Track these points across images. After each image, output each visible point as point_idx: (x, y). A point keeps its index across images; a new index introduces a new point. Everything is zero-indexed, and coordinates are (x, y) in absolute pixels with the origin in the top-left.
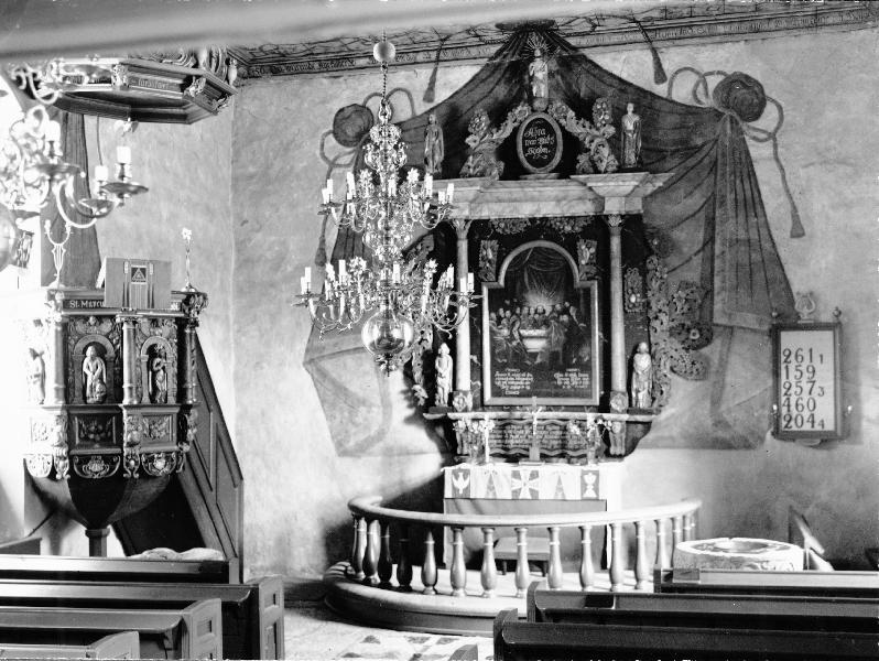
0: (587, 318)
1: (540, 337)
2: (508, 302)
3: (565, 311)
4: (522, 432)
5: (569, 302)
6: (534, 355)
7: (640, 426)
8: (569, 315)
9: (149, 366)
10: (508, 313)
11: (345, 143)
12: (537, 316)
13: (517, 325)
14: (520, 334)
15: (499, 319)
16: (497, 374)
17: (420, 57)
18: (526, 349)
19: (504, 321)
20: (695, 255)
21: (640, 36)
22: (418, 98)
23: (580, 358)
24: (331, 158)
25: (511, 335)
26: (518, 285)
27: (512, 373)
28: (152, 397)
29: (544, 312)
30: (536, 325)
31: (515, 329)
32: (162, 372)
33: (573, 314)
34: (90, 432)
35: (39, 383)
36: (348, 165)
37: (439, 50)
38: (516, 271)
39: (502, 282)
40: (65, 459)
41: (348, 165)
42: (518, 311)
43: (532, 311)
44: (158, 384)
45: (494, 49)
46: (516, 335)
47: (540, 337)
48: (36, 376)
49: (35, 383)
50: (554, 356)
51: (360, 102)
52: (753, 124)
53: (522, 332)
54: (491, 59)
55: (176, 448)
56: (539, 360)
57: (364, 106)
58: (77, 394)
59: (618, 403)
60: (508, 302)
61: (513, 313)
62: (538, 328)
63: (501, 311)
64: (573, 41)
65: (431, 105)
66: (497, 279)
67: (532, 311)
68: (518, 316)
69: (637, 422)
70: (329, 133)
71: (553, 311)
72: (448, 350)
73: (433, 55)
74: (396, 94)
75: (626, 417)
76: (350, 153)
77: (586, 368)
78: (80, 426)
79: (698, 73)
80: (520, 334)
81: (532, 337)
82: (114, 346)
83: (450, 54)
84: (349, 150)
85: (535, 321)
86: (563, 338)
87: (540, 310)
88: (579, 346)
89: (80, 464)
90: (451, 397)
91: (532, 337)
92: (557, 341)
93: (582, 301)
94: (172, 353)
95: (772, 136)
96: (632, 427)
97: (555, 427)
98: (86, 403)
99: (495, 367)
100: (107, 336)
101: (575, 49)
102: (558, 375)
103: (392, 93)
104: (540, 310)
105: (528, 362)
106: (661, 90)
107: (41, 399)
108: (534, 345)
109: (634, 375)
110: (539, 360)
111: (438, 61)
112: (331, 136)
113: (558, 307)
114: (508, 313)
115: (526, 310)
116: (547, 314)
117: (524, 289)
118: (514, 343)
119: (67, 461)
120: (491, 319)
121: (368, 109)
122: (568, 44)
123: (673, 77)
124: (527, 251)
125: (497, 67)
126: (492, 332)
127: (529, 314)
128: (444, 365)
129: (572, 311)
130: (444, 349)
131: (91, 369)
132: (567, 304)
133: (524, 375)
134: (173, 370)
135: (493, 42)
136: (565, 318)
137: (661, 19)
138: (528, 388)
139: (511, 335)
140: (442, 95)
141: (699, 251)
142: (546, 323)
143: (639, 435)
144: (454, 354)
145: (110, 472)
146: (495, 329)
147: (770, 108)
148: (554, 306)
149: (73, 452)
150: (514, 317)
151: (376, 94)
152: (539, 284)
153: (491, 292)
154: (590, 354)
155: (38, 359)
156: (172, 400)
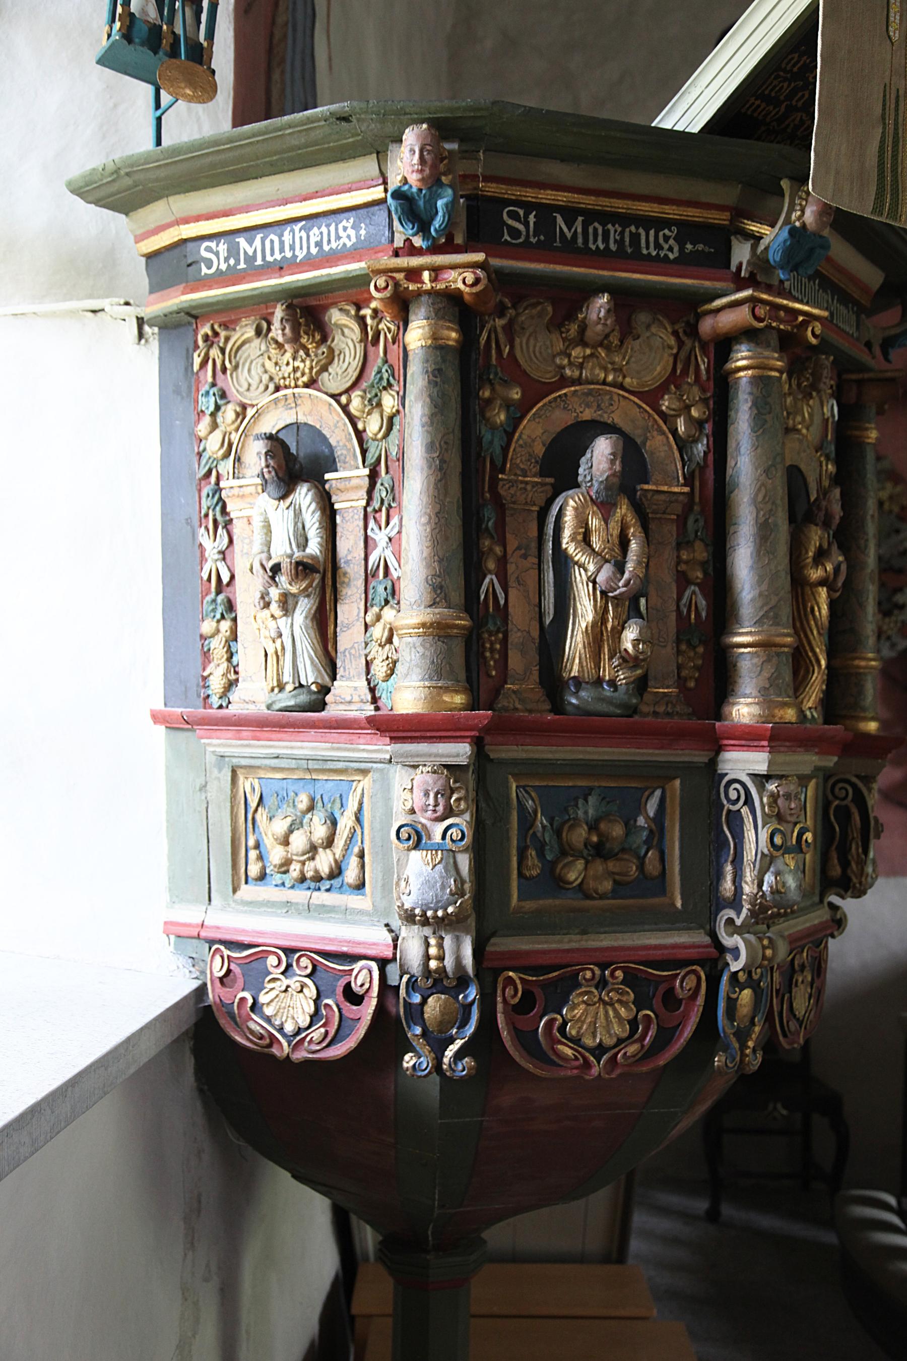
34: (565, 851)
35: (304, 608)
40: (462, 982)
48: (303, 569)
49: (287, 604)
58: (515, 661)
78: (527, 822)
82: (683, 445)
89: (526, 1004)
98: (558, 707)
100: (651, 397)
107: (310, 675)
119: (472, 993)
131: (597, 544)
145: (665, 1037)
149: (501, 944)
155: (304, 495)
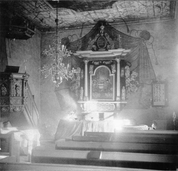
0: (112, 83)
1: (102, 86)
3: (108, 80)
6: (101, 89)
9: (16, 89)
13: (97, 83)
15: (94, 82)
16: (93, 93)
17: (79, 27)
18: (99, 88)
19: (95, 82)
21: (124, 23)
22: (79, 36)
23: (110, 90)
25: (96, 85)
28: (16, 95)
30: (101, 83)
32: (18, 90)
37: (82, 26)
39: (94, 74)
43: (101, 80)
44: (17, 92)
45: (94, 26)
46: (97, 85)
47: (102, 86)
50: (105, 90)
52: (147, 41)
54: (93, 28)
55: (21, 106)
56: (102, 91)
59: (118, 99)
60: (95, 78)
61: (97, 81)
62: (102, 84)
64: (110, 24)
65: (81, 38)
67: (101, 80)
68: (98, 82)
69: (123, 104)
73: (81, 27)
74: (74, 35)
75: (120, 102)
77: (111, 92)
79: (136, 31)
80: (98, 85)
81: (100, 86)
83: (85, 27)
85: (101, 82)
88: (111, 88)
91: (100, 86)
93: (111, 78)
94: (21, 86)
95: (151, 44)
101: (110, 25)
102: (106, 94)
104: (102, 80)
106: (128, 34)
108: (101, 87)
110: (102, 91)
111: (82, 28)
113: (106, 79)
114: (96, 81)
115: (99, 80)
118: (97, 87)
120: (92, 81)
122: (109, 24)
123: (131, 31)
125: (94, 29)
126: (92, 85)
128: (82, 91)
129: (109, 80)
130: (82, 88)
132: (108, 79)
134: (21, 90)
135: (93, 24)
136: (108, 82)
137: (128, 19)
139: (96, 85)
140: (83, 36)
142: (103, 83)
144: (84, 89)
147: (151, 38)
148: (105, 79)
150: (97, 81)
153: (92, 76)
154: (112, 89)
156: (21, 96)
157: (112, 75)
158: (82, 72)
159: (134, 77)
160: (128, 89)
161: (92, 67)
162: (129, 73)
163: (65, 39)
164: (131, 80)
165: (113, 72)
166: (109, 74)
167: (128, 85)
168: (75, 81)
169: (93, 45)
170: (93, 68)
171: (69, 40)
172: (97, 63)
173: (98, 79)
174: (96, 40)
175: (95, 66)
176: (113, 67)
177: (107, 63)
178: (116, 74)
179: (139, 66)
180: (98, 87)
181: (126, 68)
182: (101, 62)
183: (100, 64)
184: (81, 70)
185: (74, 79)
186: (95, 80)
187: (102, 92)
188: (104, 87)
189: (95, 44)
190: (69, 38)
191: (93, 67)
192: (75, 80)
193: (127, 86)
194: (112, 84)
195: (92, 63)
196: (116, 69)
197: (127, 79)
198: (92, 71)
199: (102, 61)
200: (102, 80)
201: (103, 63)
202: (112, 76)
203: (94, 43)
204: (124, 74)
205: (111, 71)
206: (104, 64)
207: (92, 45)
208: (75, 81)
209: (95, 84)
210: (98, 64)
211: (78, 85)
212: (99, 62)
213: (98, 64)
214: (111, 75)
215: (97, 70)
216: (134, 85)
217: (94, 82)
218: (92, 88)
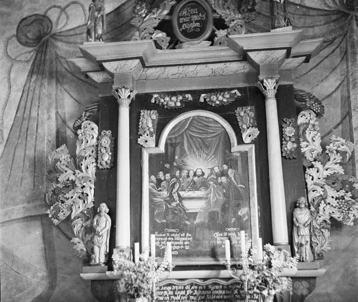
0: (246, 180)
1: (200, 198)
2: (167, 166)
3: (223, 174)
4: (184, 293)
5: (227, 164)
7: (305, 284)
8: (227, 176)
10: (168, 176)
11: (26, 44)
12: (196, 179)
13: (177, 186)
14: (179, 196)
15: (159, 182)
19: (163, 184)
20: (335, 128)
24: (13, 57)
26: (178, 149)
27: (171, 233)
29: (203, 174)
30: (194, 186)
31: (174, 190)
33: (232, 176)
36: (27, 61)
38: (176, 138)
39: (162, 149)
41: (27, 61)
42: (177, 173)
46: (175, 196)
47: (200, 198)
50: (212, 216)
51: (42, 13)
53: (181, 193)
56: (198, 221)
57: (44, 16)
60: (167, 166)
61: (173, 176)
63: (161, 175)
66: (157, 145)
70: (13, 36)
71: (212, 173)
72: (108, 210)
74: (72, 6)
76: (30, 52)
80: (179, 196)
84: (31, 49)
85: (194, 183)
86: (221, 198)
87: (199, 173)
88: (238, 206)
90: (109, 255)
92: (216, 202)
96: (297, 283)
97: (217, 287)
99: (154, 228)
103: (68, 5)
104: (199, 173)
105: (187, 222)
108: (192, 207)
109: (295, 229)
110: (198, 221)
112: (14, 38)
113: (217, 170)
115: (185, 173)
116: (206, 176)
117: (183, 154)
118: (174, 204)
120: (151, 181)
121: (48, 17)
124: (187, 120)
126: (151, 194)
127: (188, 176)
128: (104, 223)
129: (231, 172)
130: (104, 208)
132: (225, 167)
133: (183, 235)
136: (224, 179)
138: (187, 248)
139: (171, 196)
141: (338, 125)
142: (205, 185)
143: (305, 292)
144: (113, 214)
146: (155, 191)
148: (212, 169)
151: (55, 6)
152: (198, 149)
153: (151, 157)
157: (243, 148)
158: (106, 141)
159: (339, 158)
160: (321, 208)
161: (149, 119)
162: (318, 141)
163: (35, 20)
164: (326, 173)
165: (244, 136)
166: (228, 144)
167: (320, 191)
168: (73, 182)
169: (155, 28)
170: (153, 120)
171: (51, 21)
172: (174, 102)
173: (181, 169)
174: (166, 12)
175: (167, 114)
176: (245, 115)
177: (218, 99)
178: (262, 143)
179: (351, 118)
180: (178, 205)
181: (301, 120)
182: (189, 97)
183: (188, 106)
184: (100, 134)
185: (70, 172)
186: (164, 175)
187: (198, 225)
188: (209, 203)
189: (165, 26)
190: (53, 15)
191: (154, 117)
192: (72, 177)
193: (311, 195)
194: (247, 190)
195: (153, 101)
196: (261, 122)
197: (312, 166)
198: (151, 134)
199: (196, 93)
200: (195, 175)
201: (202, 100)
202: (245, 155)
203: (157, 22)
204: (295, 145)
205: (238, 132)
206: (205, 106)
207: (152, 31)
208: (73, 182)
209: (165, 194)
210: (179, 104)
211: (83, 197)
212: (180, 98)
213: (179, 104)
214: (236, 148)
215: (174, 128)
216: (342, 193)
217: (159, 182)
218: (152, 211)
